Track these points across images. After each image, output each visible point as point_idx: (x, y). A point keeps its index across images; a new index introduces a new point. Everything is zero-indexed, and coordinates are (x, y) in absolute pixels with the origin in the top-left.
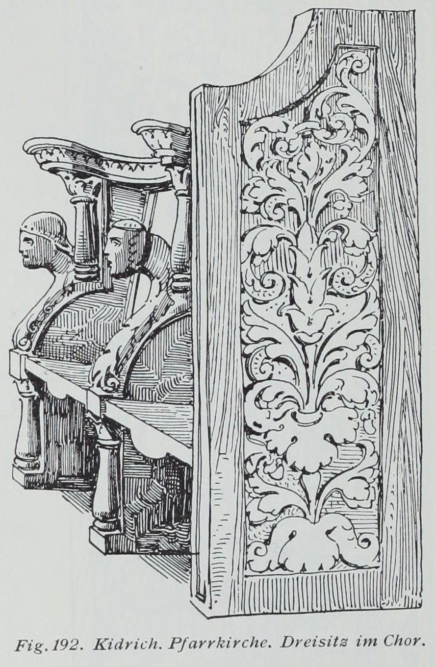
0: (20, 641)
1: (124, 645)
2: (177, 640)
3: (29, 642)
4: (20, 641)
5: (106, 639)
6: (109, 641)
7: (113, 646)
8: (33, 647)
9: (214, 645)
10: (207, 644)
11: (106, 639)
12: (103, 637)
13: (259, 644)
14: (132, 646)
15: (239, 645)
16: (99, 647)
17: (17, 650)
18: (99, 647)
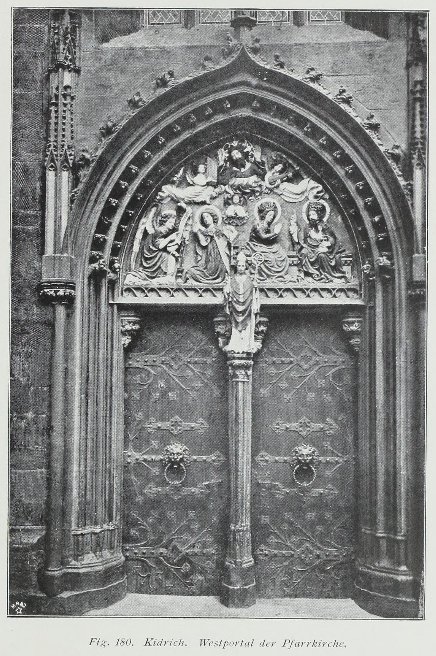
0: (92, 639)
1: (163, 643)
2: (287, 641)
3: (98, 640)
4: (92, 639)
5: (152, 639)
6: (153, 641)
7: (156, 643)
8: (100, 643)
9: (311, 645)
10: (306, 644)
11: (152, 639)
12: (150, 638)
13: (339, 645)
14: (168, 644)
15: (326, 645)
16: (148, 644)
17: (90, 644)
18: (148, 644)
